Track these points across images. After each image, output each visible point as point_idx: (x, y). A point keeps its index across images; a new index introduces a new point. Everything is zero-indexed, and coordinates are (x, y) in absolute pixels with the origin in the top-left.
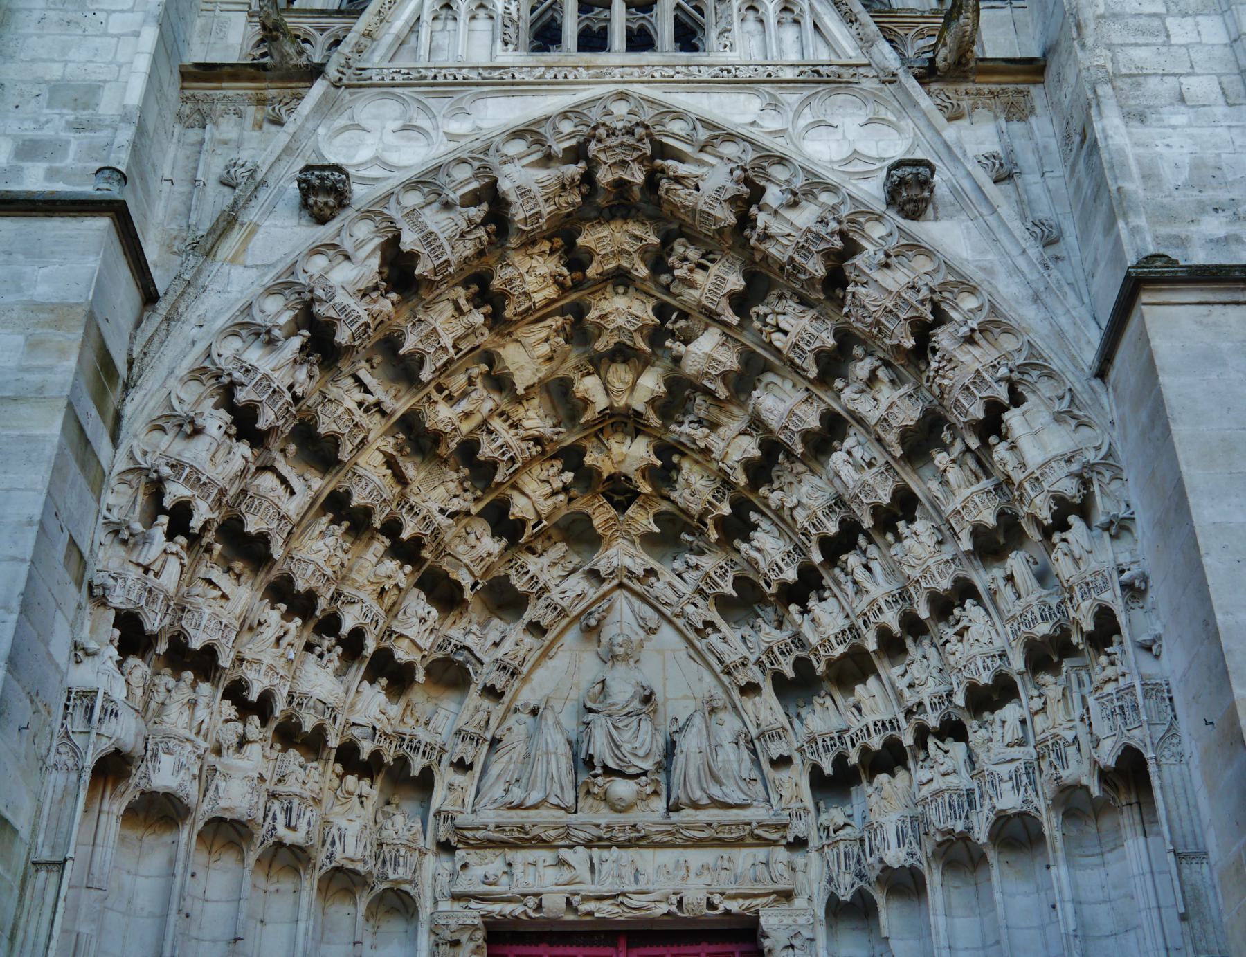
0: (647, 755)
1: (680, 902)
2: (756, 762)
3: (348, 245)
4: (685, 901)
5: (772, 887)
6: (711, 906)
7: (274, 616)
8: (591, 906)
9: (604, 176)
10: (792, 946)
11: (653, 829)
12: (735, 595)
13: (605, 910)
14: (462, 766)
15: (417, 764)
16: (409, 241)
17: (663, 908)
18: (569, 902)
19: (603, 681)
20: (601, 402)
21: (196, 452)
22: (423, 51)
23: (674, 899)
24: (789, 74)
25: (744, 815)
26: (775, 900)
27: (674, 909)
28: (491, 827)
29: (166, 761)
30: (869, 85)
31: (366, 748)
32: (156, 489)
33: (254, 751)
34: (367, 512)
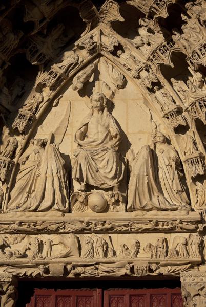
0: (114, 178)
1: (132, 269)
2: (183, 179)
4: (135, 268)
5: (187, 260)
6: (151, 270)
8: (78, 270)
10: (199, 295)
11: (117, 224)
12: (172, 66)
13: (88, 272)
17: (123, 272)
18: (65, 267)
19: (87, 125)
23: (128, 266)
25: (171, 215)
26: (190, 267)
27: (128, 272)
28: (18, 222)
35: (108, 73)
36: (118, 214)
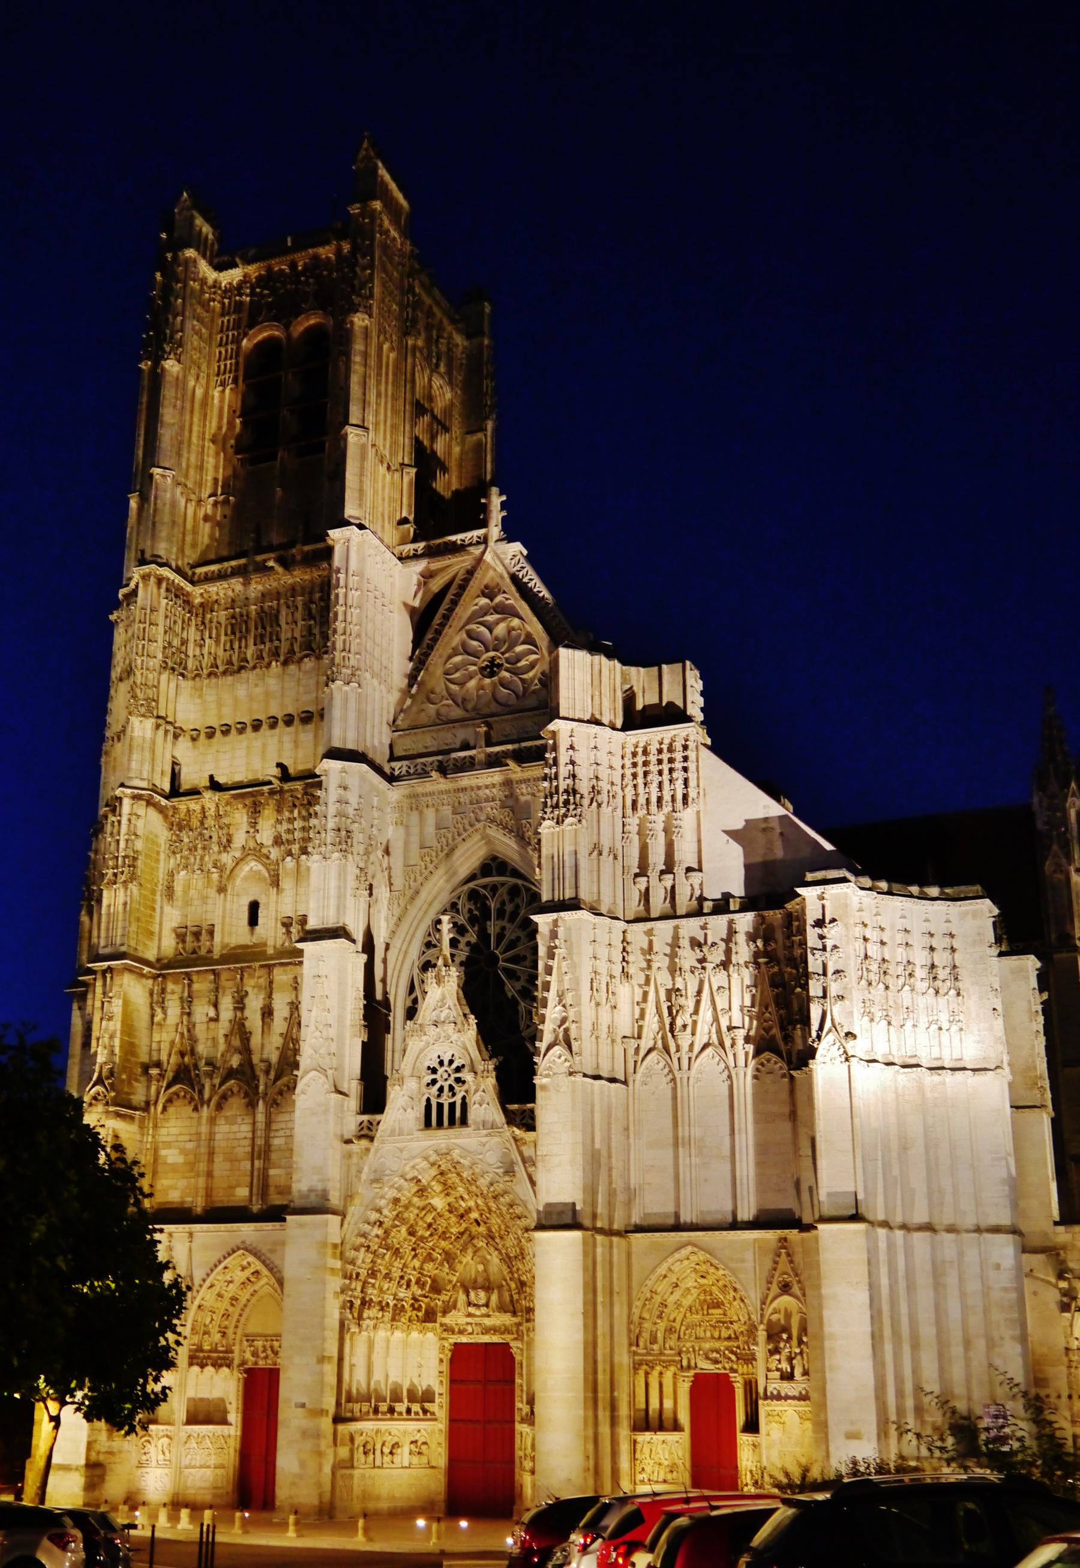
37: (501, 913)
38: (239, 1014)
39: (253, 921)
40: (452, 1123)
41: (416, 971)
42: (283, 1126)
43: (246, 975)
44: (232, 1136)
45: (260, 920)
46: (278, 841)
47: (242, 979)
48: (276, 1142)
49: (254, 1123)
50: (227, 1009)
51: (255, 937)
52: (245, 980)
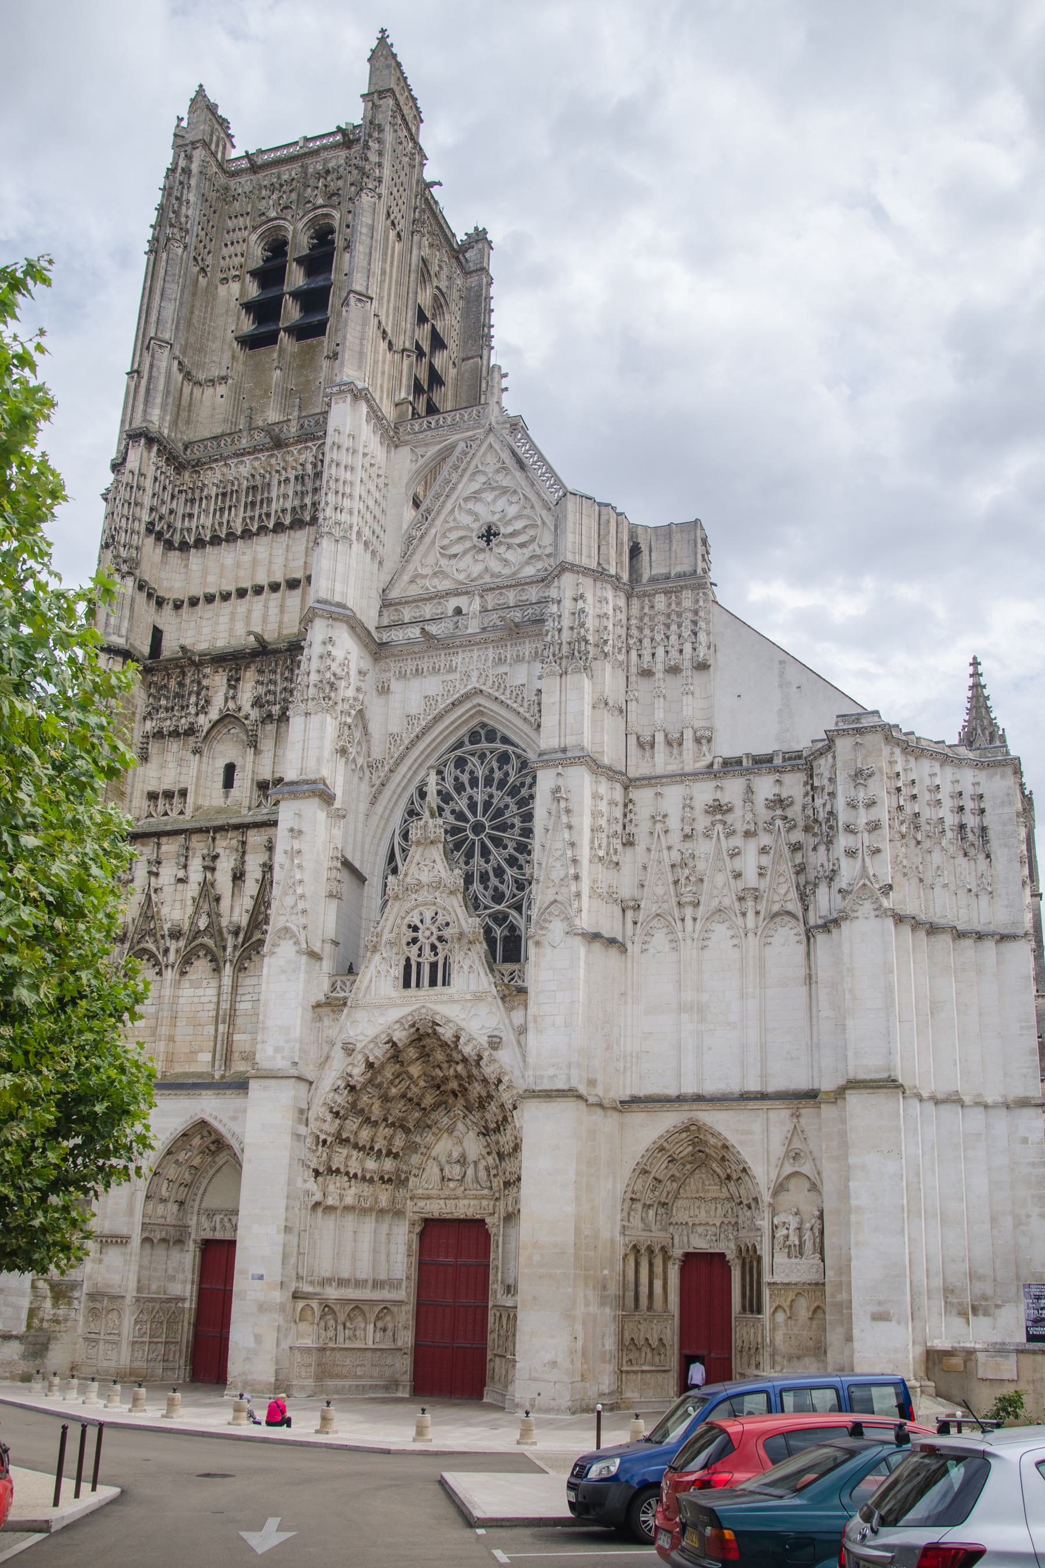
2: (489, 1175)
3: (356, 1063)
7: (355, 1153)
9: (421, 1031)
13: (448, 1217)
14: (415, 1175)
15: (403, 1176)
16: (371, 1059)
20: (441, 1075)
21: (326, 1127)
22: (373, 993)
24: (468, 997)
29: (330, 1198)
30: (490, 999)
31: (386, 1177)
32: (318, 1137)
33: (353, 1188)
34: (376, 1122)
35: (460, 1126)
36: (459, 1192)
37: (489, 781)
38: (209, 875)
39: (228, 783)
40: (433, 983)
41: (397, 839)
42: (251, 990)
43: (218, 836)
44: (196, 1000)
45: (236, 783)
46: (257, 703)
47: (214, 839)
48: (243, 1006)
49: (220, 986)
50: (196, 872)
51: (229, 800)
52: (217, 842)
